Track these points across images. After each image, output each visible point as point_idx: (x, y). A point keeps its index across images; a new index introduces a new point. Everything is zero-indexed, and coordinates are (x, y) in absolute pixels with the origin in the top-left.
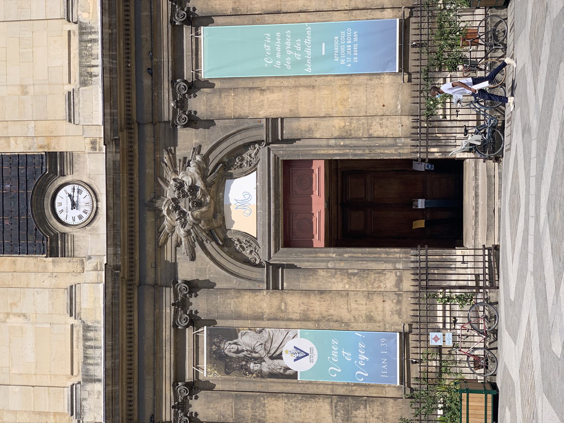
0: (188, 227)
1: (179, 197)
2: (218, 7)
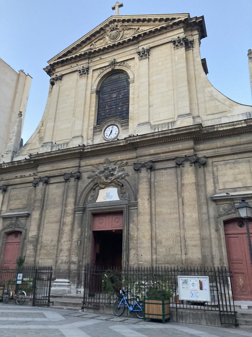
0: (98, 174)
2: (185, 177)
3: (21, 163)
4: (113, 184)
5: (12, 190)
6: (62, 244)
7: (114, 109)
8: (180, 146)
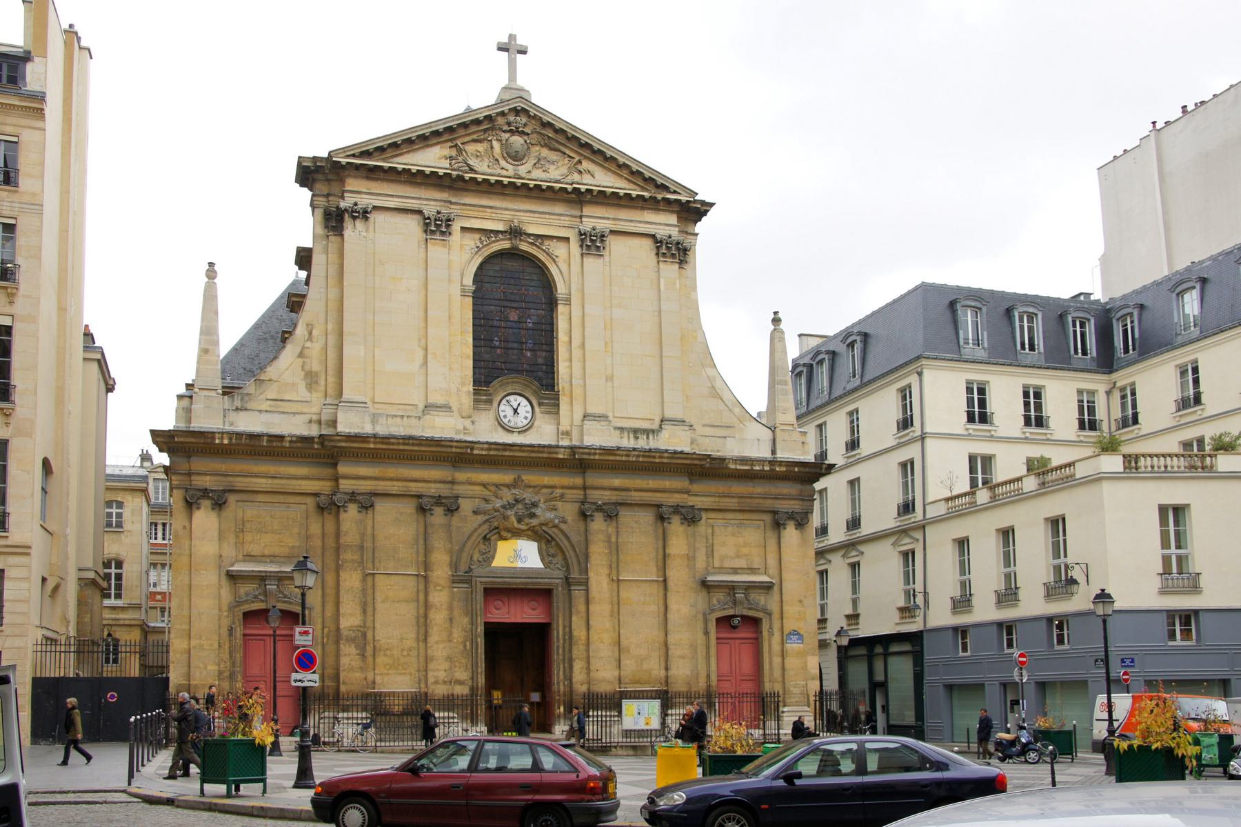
0: (500, 509)
1: (526, 504)
2: (670, 542)
4: (529, 533)
5: (240, 504)
6: (431, 647)
7: (515, 351)
8: (667, 483)
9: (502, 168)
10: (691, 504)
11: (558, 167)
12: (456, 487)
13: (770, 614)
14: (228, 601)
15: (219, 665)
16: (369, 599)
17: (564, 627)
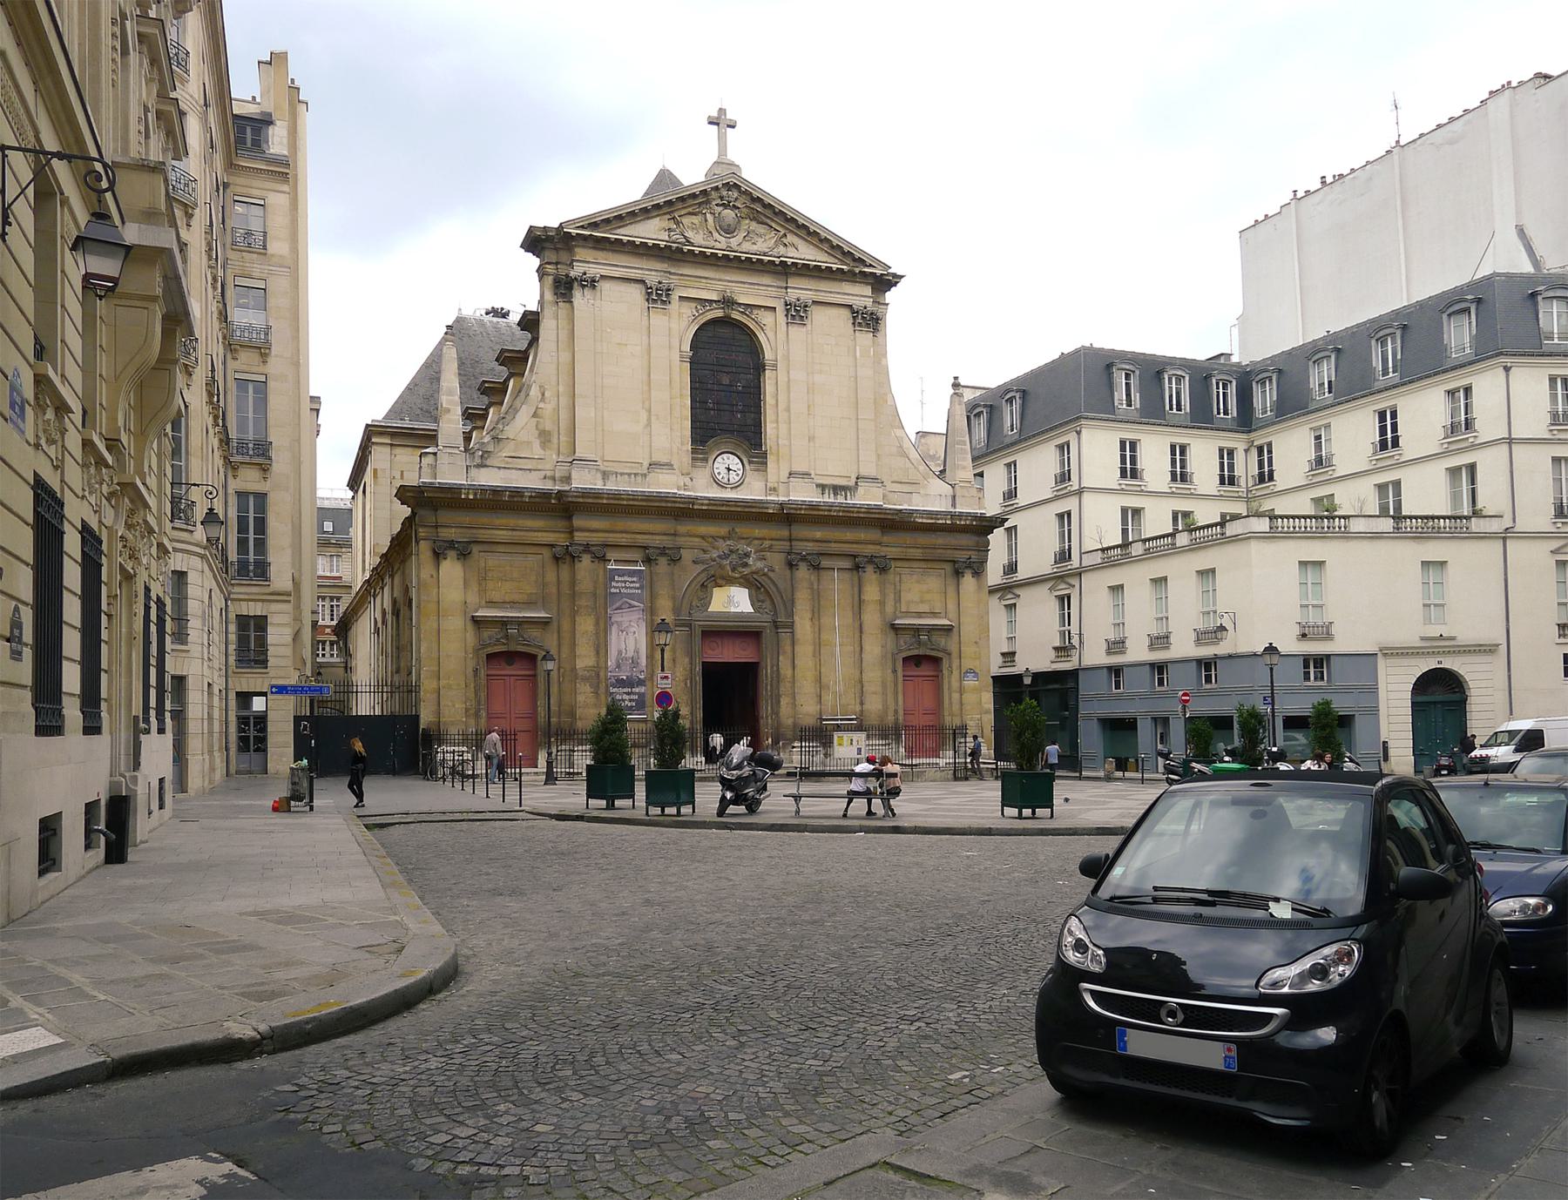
3: (523, 496)
4: (741, 580)
7: (727, 413)
8: (862, 535)
9: (716, 241)
10: (883, 554)
11: (765, 240)
12: (678, 538)
13: (949, 654)
14: (473, 645)
15: (465, 703)
16: (602, 641)
17: (772, 667)
